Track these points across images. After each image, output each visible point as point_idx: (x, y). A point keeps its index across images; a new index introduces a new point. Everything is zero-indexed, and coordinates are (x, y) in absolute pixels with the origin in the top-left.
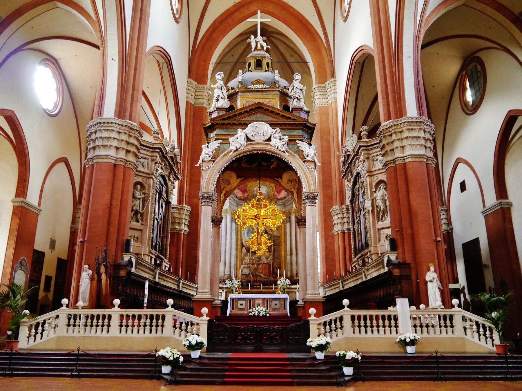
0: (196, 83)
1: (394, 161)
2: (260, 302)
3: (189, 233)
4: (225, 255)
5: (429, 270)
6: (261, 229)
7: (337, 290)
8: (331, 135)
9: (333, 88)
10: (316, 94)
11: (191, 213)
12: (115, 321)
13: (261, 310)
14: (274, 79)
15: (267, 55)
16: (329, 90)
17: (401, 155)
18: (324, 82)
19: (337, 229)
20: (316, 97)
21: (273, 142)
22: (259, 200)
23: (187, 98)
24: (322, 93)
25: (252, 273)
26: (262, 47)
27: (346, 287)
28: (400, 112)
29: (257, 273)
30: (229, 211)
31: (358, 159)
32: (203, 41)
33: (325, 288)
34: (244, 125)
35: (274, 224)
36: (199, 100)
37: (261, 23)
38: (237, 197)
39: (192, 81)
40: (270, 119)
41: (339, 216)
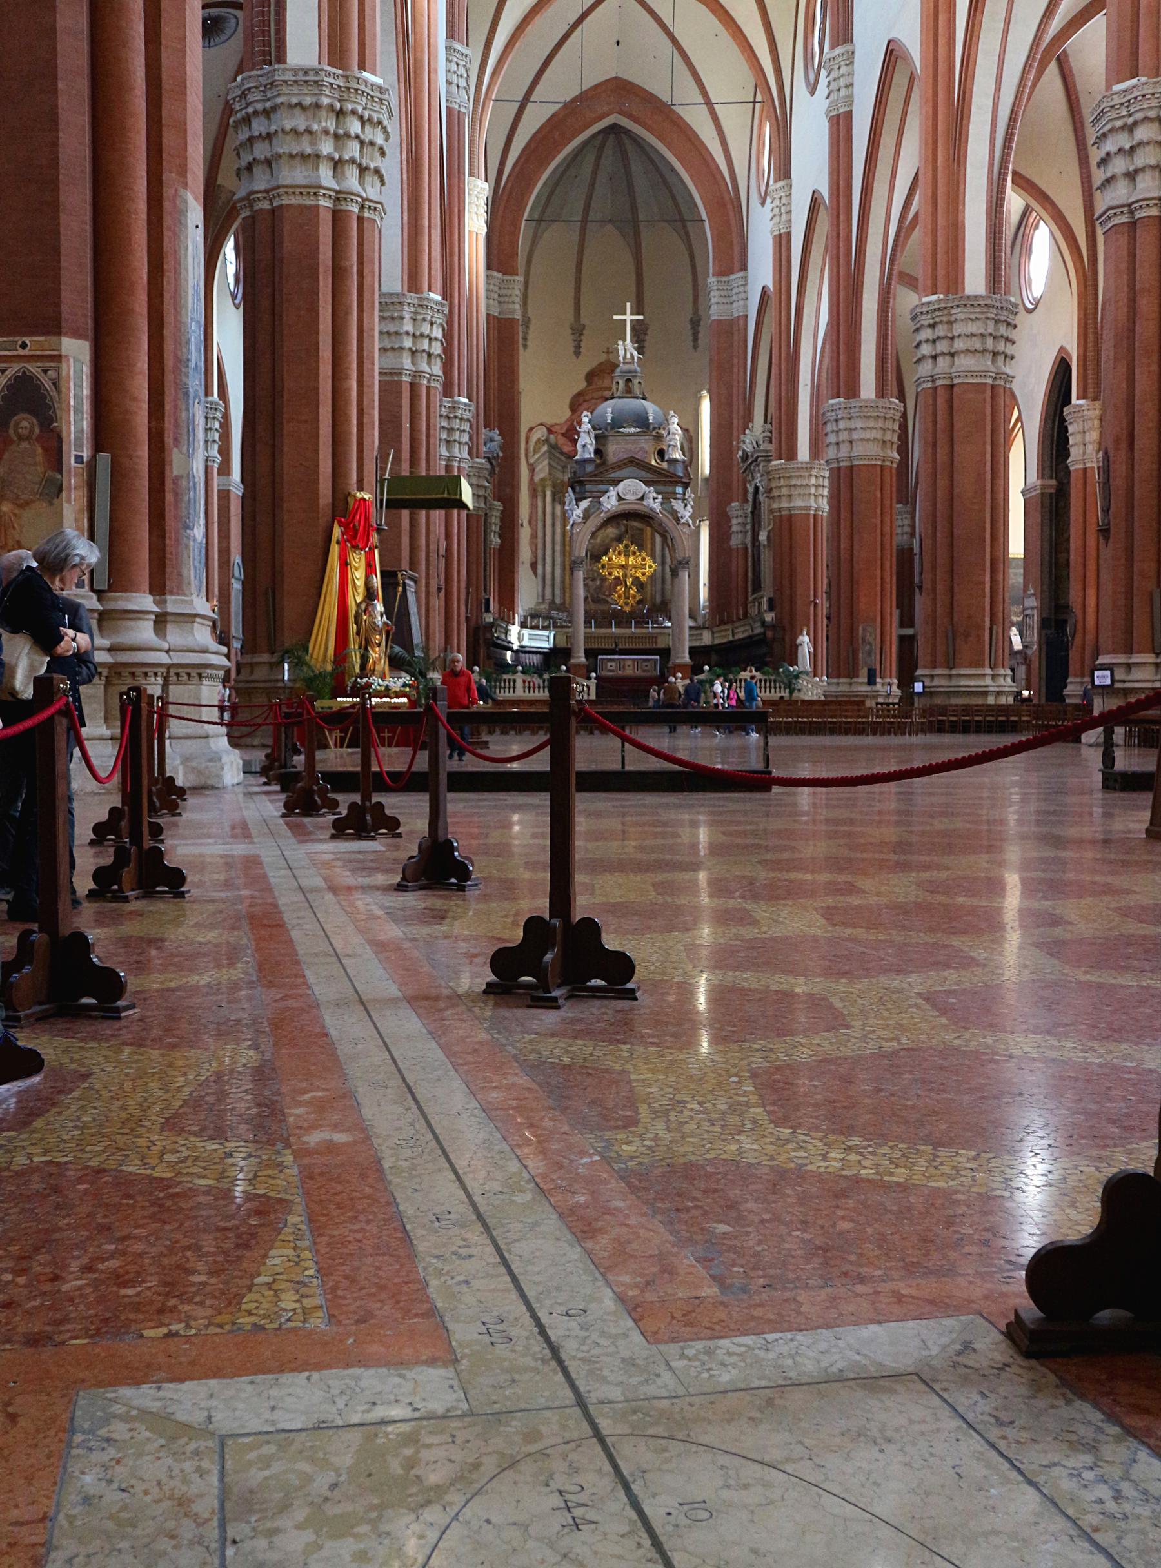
0: (499, 275)
1: (780, 510)
2: (630, 663)
3: (502, 545)
4: (544, 565)
5: (801, 634)
6: (629, 581)
7: (725, 640)
8: (735, 376)
9: (741, 289)
10: (712, 294)
11: (502, 512)
12: (519, 683)
13: (629, 672)
14: (647, 418)
15: (638, 369)
16: (736, 290)
17: (786, 505)
18: (728, 275)
19: (735, 541)
20: (713, 300)
21: (645, 503)
22: (626, 546)
23: (488, 307)
24: (723, 293)
25: (592, 596)
26: (632, 355)
27: (737, 637)
28: (791, 454)
29: (601, 596)
30: (549, 482)
31: (758, 465)
32: (509, 185)
33: (713, 633)
34: (616, 482)
35: (644, 574)
36: (505, 306)
37: (632, 321)
38: (562, 453)
39: (495, 274)
40: (643, 474)
41: (740, 520)
